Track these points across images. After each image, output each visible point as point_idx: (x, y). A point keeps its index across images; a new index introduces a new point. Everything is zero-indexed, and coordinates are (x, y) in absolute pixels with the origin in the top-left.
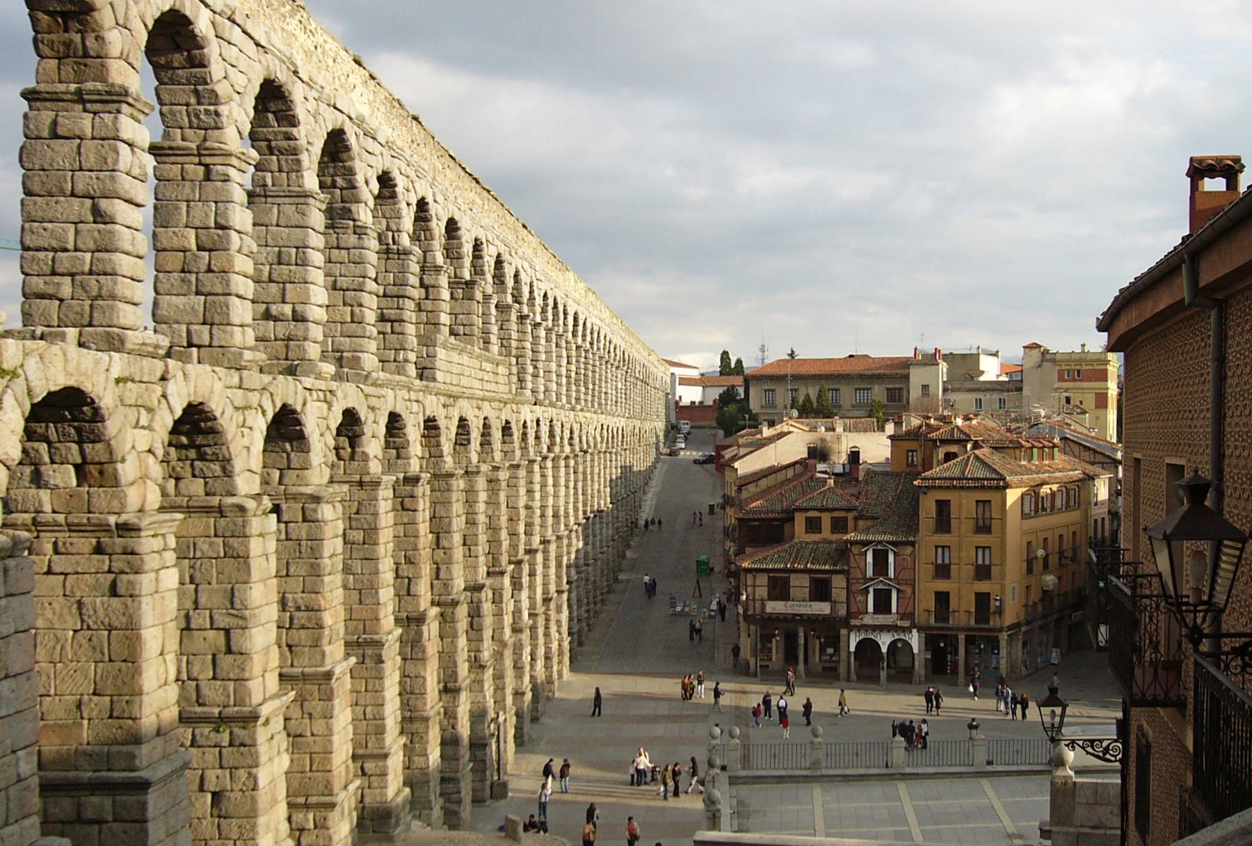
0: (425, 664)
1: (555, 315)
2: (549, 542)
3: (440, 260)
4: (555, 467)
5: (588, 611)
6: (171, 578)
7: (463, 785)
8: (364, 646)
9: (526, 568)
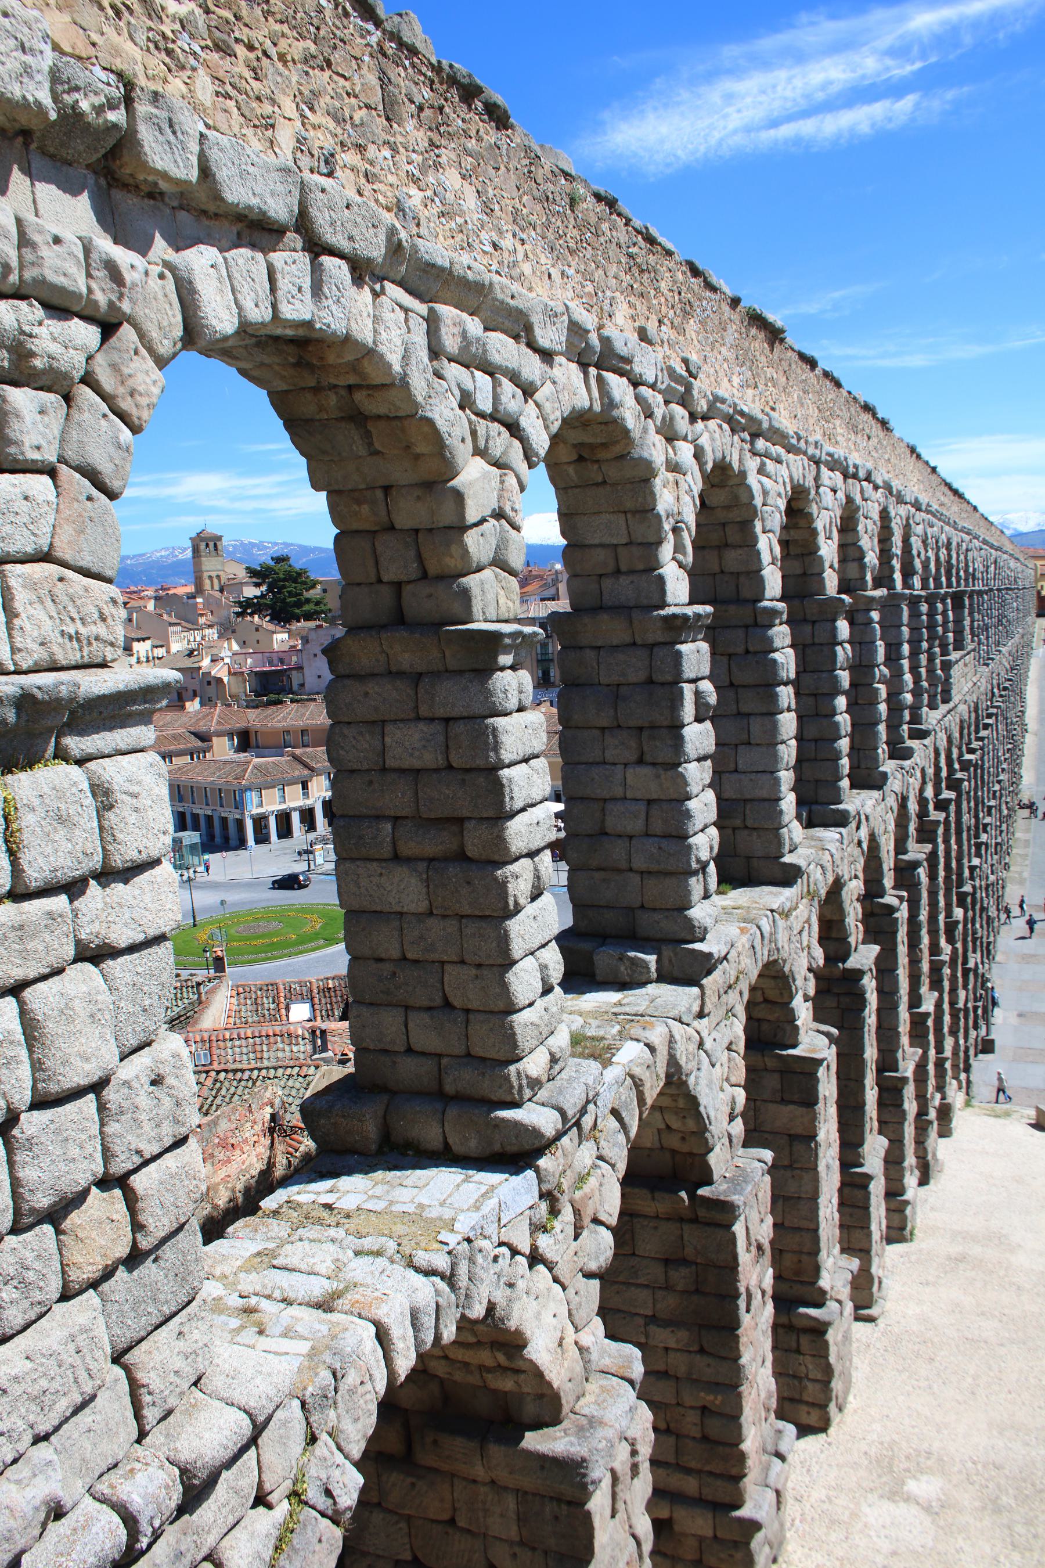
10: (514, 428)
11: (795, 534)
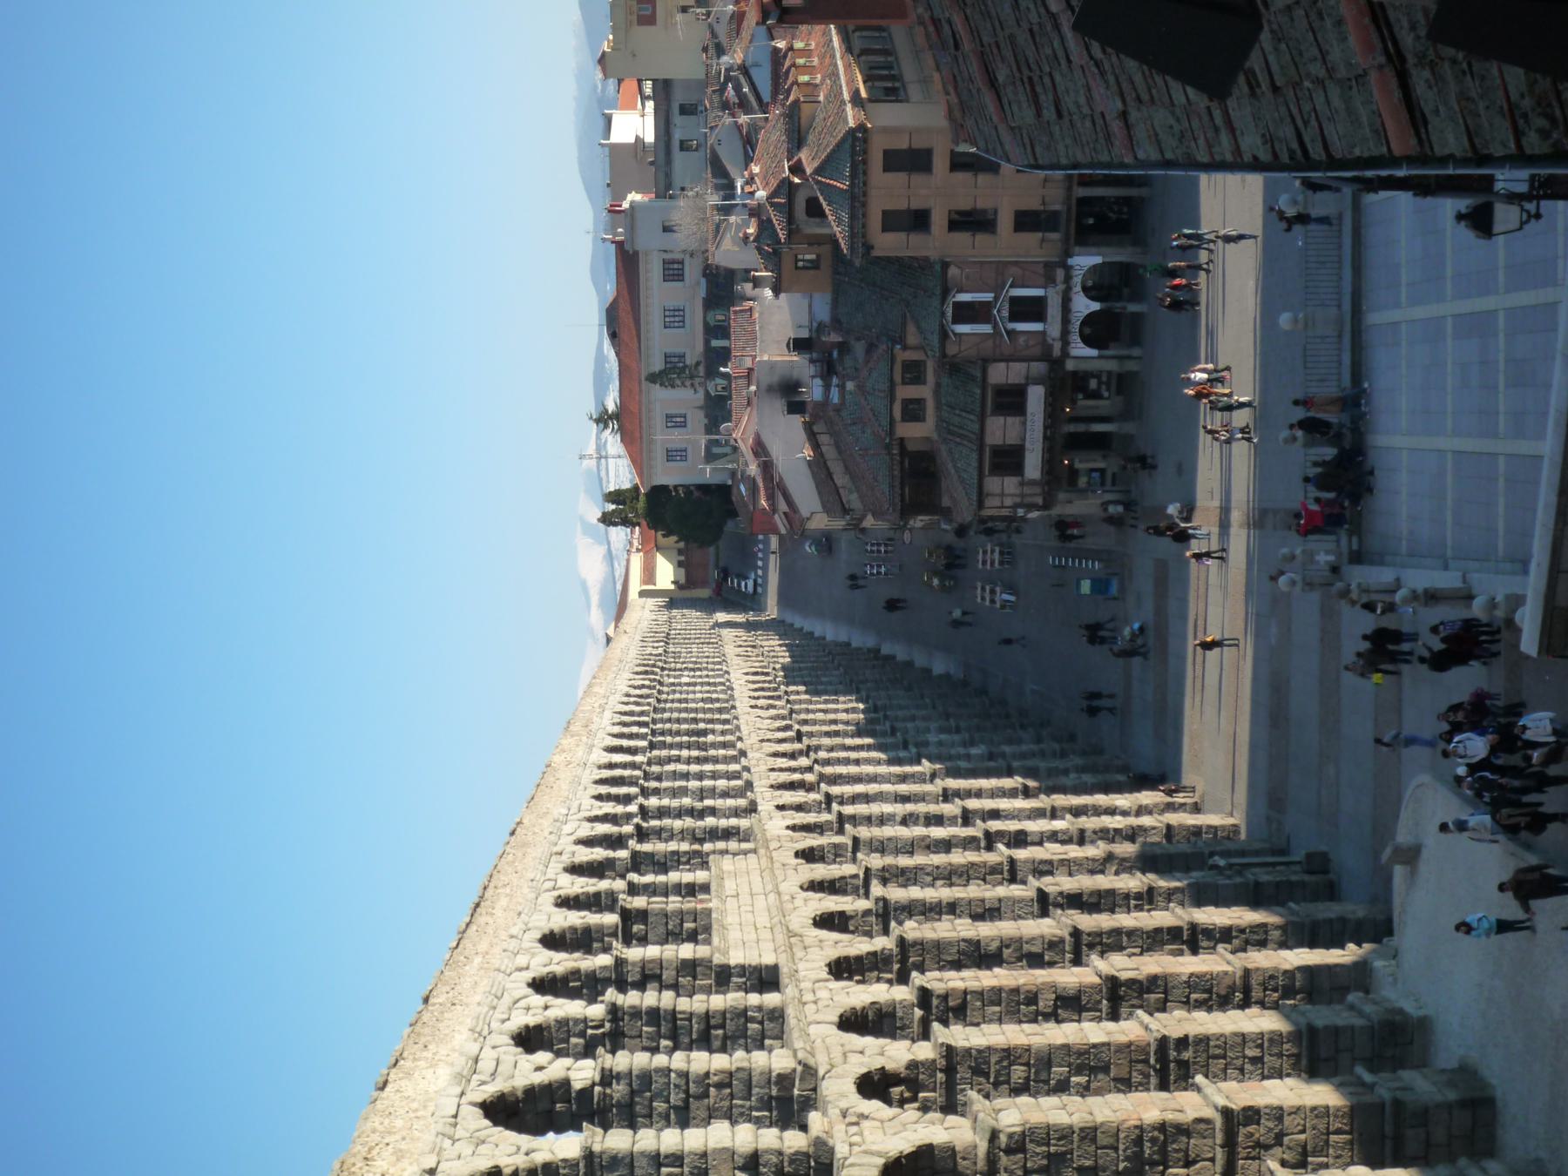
0: (1171, 975)
2: (945, 790)
3: (603, 960)
4: (835, 780)
5: (1022, 727)
7: (1321, 916)
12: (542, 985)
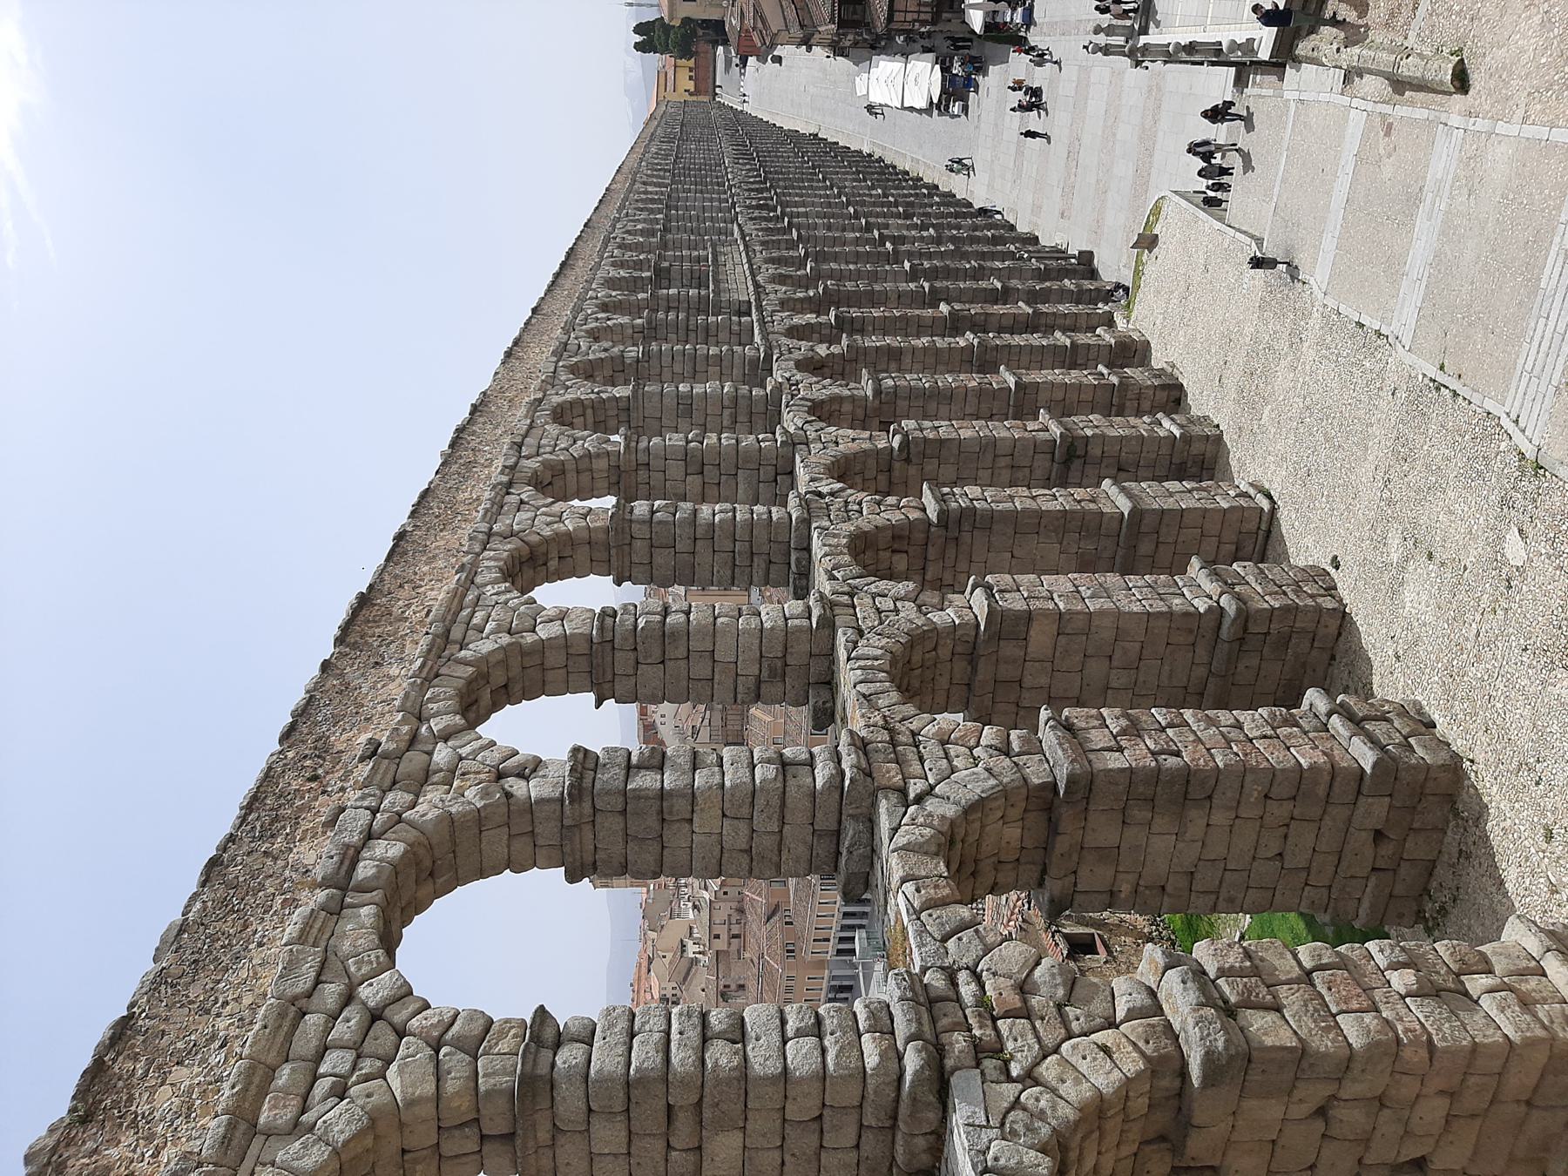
1: (653, 201)
3: (640, 296)
4: (788, 204)
6: (973, 491)
8: (985, 362)
9: (885, 232)
10: (375, 1016)
11: (554, 554)
12: (604, 307)
